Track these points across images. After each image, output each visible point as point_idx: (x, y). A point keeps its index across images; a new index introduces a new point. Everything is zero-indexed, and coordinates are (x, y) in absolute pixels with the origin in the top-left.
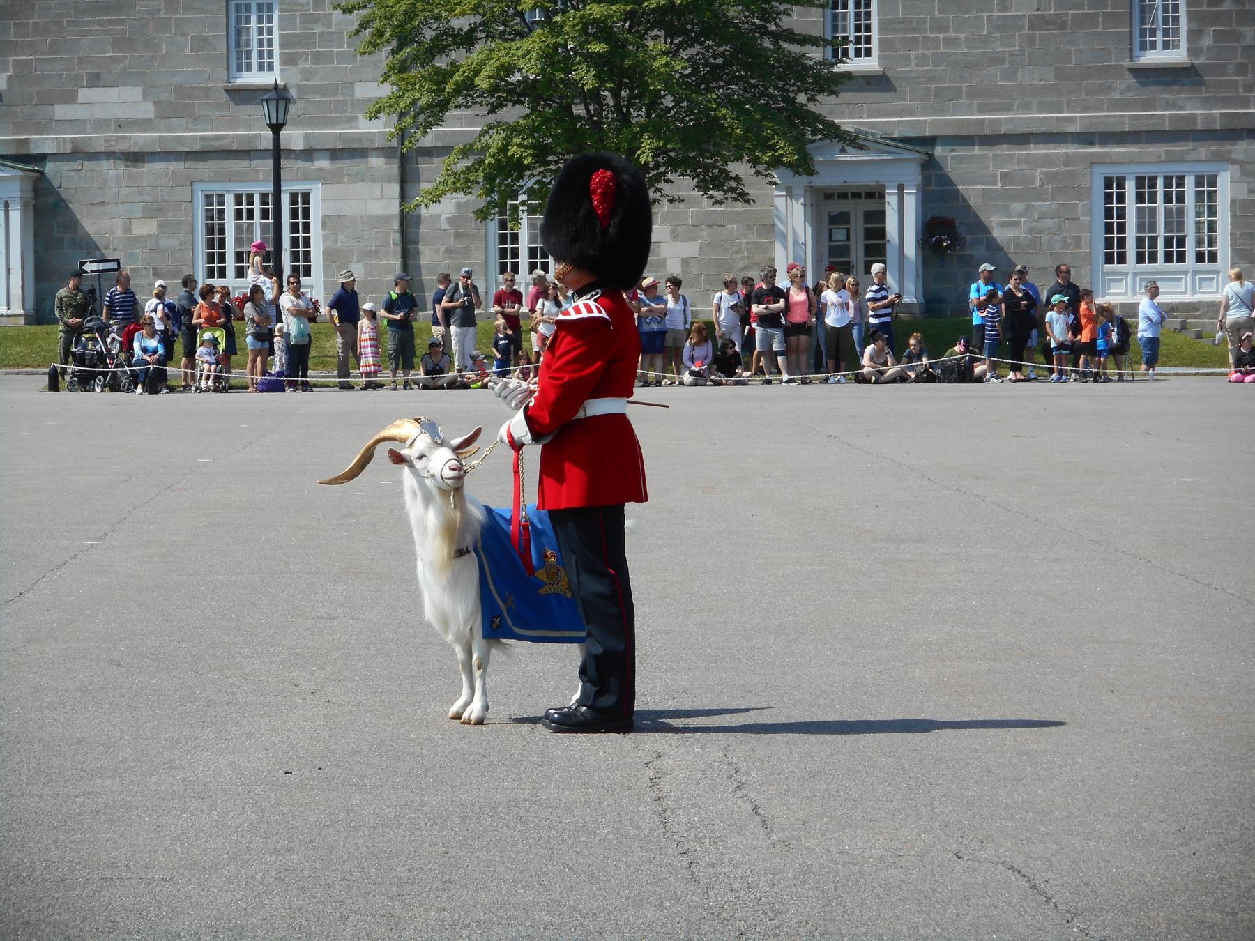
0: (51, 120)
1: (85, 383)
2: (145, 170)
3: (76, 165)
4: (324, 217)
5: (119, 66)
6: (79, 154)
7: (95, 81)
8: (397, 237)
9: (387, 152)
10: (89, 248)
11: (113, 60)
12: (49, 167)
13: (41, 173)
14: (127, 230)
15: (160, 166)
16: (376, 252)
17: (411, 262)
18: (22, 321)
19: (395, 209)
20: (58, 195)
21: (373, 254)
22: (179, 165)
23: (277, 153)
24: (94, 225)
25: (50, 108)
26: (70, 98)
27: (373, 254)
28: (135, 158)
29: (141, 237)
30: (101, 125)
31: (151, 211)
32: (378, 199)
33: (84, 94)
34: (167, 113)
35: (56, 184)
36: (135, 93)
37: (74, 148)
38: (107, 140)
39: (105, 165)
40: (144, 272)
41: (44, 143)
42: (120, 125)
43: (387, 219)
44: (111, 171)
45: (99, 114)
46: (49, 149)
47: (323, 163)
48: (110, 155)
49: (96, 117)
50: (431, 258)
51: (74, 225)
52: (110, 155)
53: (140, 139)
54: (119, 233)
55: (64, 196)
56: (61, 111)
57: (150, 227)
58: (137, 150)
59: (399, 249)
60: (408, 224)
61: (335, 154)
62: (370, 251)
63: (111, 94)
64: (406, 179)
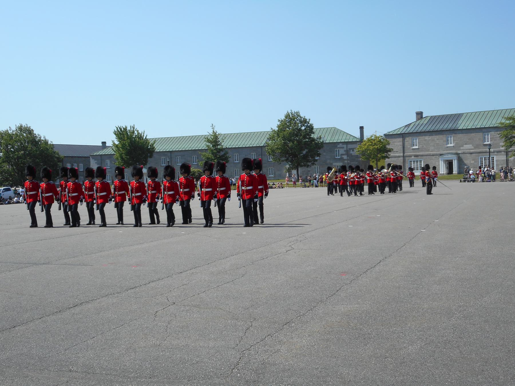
1: (465, 181)
6: (464, 153)
7: (466, 144)
9: (504, 152)
10: (465, 165)
23: (490, 152)
24: (466, 162)
26: (463, 146)
28: (471, 153)
30: (467, 149)
31: (473, 160)
32: (503, 157)
34: (475, 148)
36: (471, 145)
41: (459, 152)
42: (469, 149)
44: (468, 155)
47: (496, 153)
50: (510, 165)
51: (463, 162)
56: (461, 148)
57: (473, 162)
60: (507, 161)
61: (497, 152)
63: (468, 146)
64: (507, 155)
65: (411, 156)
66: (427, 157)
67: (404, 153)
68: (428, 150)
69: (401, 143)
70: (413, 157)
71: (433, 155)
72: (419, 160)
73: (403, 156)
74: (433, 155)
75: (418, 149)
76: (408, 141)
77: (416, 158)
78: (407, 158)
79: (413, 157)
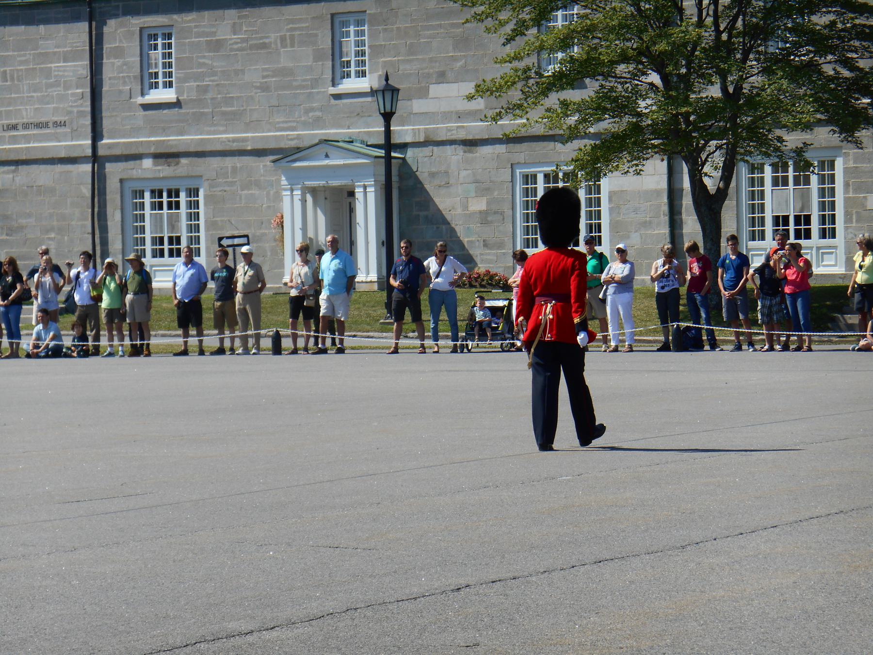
0: (411, 113)
2: (478, 154)
3: (427, 151)
4: (610, 192)
5: (459, 64)
7: (442, 78)
8: (665, 208)
11: (454, 59)
12: (410, 153)
13: (404, 159)
14: (466, 207)
15: (487, 150)
16: (650, 222)
17: (677, 232)
18: (375, 287)
19: (664, 185)
20: (417, 178)
21: (645, 224)
22: (501, 149)
24: (447, 202)
25: (409, 103)
26: (423, 93)
27: (645, 224)
28: (471, 144)
29: (475, 213)
30: (446, 116)
33: (435, 90)
35: (415, 170)
37: (426, 137)
38: (449, 130)
39: (449, 149)
40: (477, 243)
43: (658, 192)
44: (454, 155)
45: (444, 107)
46: (408, 139)
48: (452, 142)
49: (442, 110)
51: (427, 201)
52: (452, 142)
53: (476, 128)
54: (459, 211)
55: (421, 178)
58: (471, 137)
59: (667, 218)
62: (645, 222)
65: (138, 157)
66: (229, 162)
67: (96, 134)
68: (232, 119)
69: (83, 66)
70: (147, 163)
71: (259, 153)
72: (183, 186)
73: (95, 158)
74: (259, 153)
75: (178, 104)
76: (119, 53)
77: (165, 170)
78: (109, 167)
79: (147, 163)
